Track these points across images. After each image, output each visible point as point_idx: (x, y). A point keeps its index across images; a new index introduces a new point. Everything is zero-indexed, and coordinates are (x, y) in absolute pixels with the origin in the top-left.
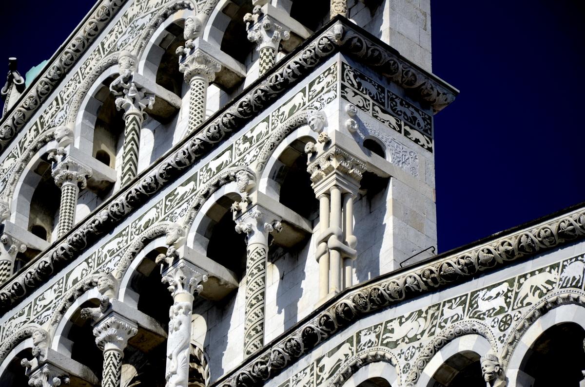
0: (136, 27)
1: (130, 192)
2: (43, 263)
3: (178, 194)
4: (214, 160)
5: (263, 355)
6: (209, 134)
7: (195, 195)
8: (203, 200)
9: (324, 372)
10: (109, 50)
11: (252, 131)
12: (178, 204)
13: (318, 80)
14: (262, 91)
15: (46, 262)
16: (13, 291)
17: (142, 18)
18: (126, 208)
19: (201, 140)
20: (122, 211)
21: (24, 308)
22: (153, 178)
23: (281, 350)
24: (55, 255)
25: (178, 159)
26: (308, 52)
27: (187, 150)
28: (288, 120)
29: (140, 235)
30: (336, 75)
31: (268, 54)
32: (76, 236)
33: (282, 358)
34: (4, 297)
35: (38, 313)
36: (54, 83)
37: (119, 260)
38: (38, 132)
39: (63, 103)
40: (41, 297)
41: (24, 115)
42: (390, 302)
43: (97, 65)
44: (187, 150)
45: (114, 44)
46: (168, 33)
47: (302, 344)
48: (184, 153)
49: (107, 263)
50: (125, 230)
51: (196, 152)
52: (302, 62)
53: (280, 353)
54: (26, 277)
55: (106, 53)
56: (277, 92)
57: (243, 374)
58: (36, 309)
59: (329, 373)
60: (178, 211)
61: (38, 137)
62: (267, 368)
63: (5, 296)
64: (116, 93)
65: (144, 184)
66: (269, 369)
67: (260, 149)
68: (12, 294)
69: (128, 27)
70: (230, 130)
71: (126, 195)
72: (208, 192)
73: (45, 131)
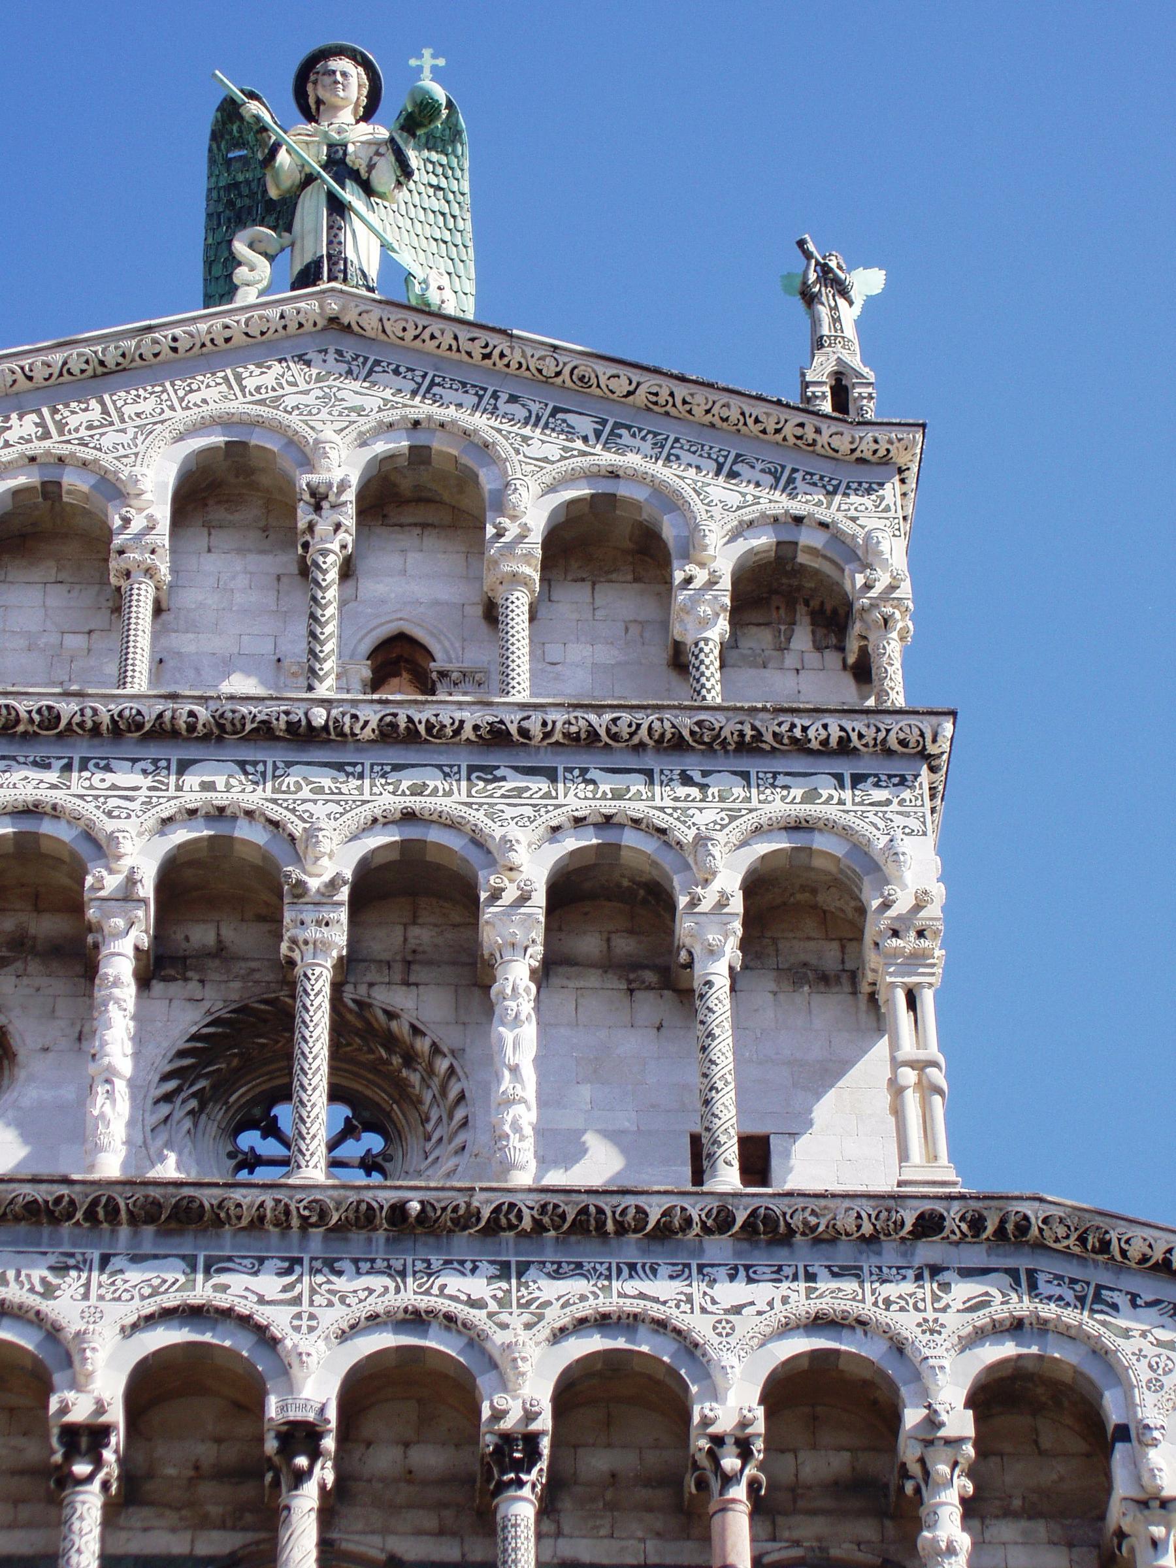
0: (337, 399)
1: (395, 715)
2: (134, 712)
3: (504, 779)
4: (601, 769)
5: (823, 1202)
6: (614, 729)
7: (557, 807)
8: (567, 825)
9: (952, 1295)
10: (258, 397)
11: (705, 774)
12: (503, 796)
13: (871, 780)
14: (754, 728)
15: (139, 713)
16: (37, 718)
17: (357, 393)
18: (368, 729)
19: (590, 725)
20: (357, 731)
21: (48, 758)
22: (457, 723)
23: (864, 1215)
24: (168, 715)
25: (525, 724)
26: (873, 729)
27: (554, 723)
28: (793, 807)
29: (402, 799)
30: (922, 795)
31: (707, 650)
32: (234, 712)
33: (859, 1227)
34: (9, 714)
35: (91, 787)
36: (100, 370)
37: (342, 814)
38: (46, 435)
39: (123, 421)
40: (102, 763)
41: (15, 381)
42: (1113, 1258)
43: (222, 406)
44: (554, 723)
45: (272, 394)
46: (407, 452)
47: (908, 1227)
48: (544, 724)
49: (304, 801)
50: (354, 765)
51: (567, 735)
52: (854, 736)
53: (859, 1217)
54: (82, 710)
55: (249, 398)
56: (777, 746)
57: (767, 1208)
58: (90, 779)
59: (964, 1303)
60: (510, 812)
61: (47, 443)
62: (818, 1225)
63: (13, 712)
64: (306, 497)
65: (433, 720)
66: (821, 1228)
67: (733, 819)
68: (31, 721)
69: (312, 386)
70: (651, 743)
71: (383, 713)
72: (585, 818)
73: (68, 442)
